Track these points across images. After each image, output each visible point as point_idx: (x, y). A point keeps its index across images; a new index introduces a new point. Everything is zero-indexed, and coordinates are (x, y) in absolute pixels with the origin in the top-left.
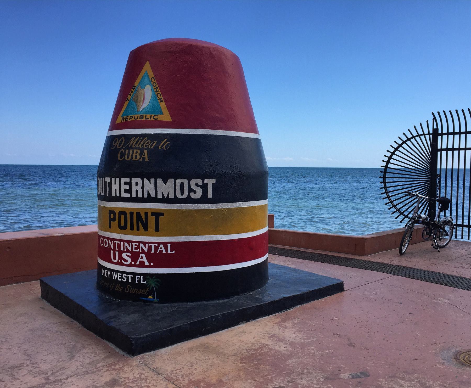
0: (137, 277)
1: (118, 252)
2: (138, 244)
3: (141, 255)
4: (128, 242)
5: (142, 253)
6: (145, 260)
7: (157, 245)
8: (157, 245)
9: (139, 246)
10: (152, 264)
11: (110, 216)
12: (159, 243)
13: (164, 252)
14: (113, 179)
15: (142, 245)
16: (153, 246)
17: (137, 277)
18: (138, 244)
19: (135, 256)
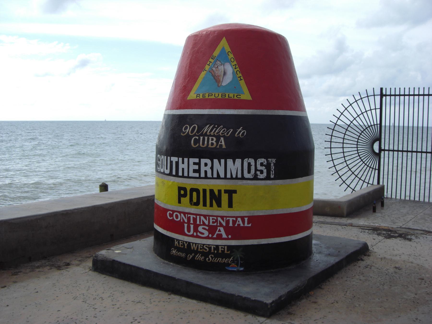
1: (193, 225)
2: (215, 218)
3: (219, 228)
4: (205, 216)
7: (234, 219)
8: (234, 219)
9: (217, 221)
11: (179, 192)
12: (237, 217)
13: (242, 225)
14: (181, 159)
15: (219, 219)
16: (231, 219)
18: (215, 218)
19: (212, 230)
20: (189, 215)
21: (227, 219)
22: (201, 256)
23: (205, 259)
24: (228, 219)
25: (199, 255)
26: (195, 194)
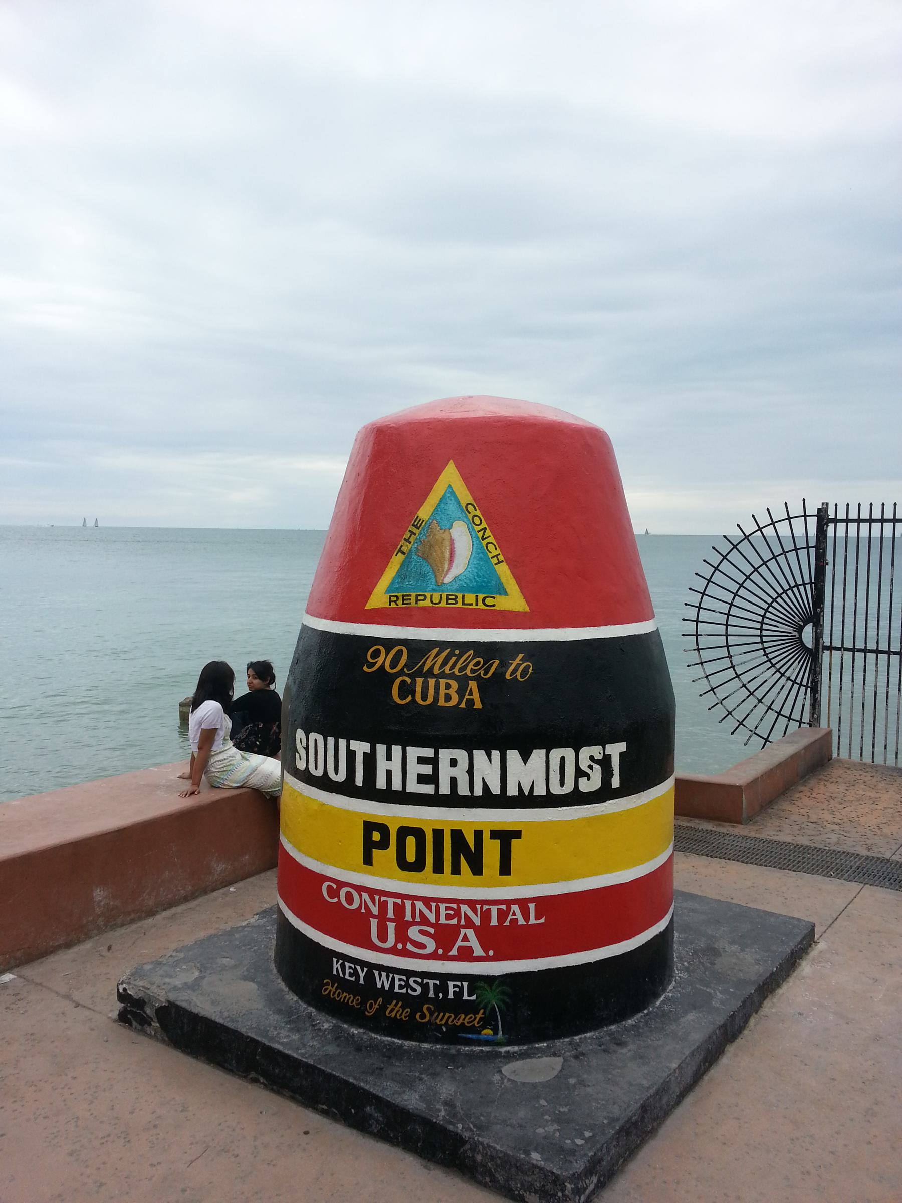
0: (451, 984)
1: (394, 924)
3: (463, 931)
5: (464, 927)
6: (474, 943)
7: (504, 907)
10: (491, 953)
17: (451, 984)
20: (383, 899)
21: (484, 909)
22: (403, 1007)
23: (412, 1016)
24: (485, 907)
25: (396, 1005)
26: (411, 841)
